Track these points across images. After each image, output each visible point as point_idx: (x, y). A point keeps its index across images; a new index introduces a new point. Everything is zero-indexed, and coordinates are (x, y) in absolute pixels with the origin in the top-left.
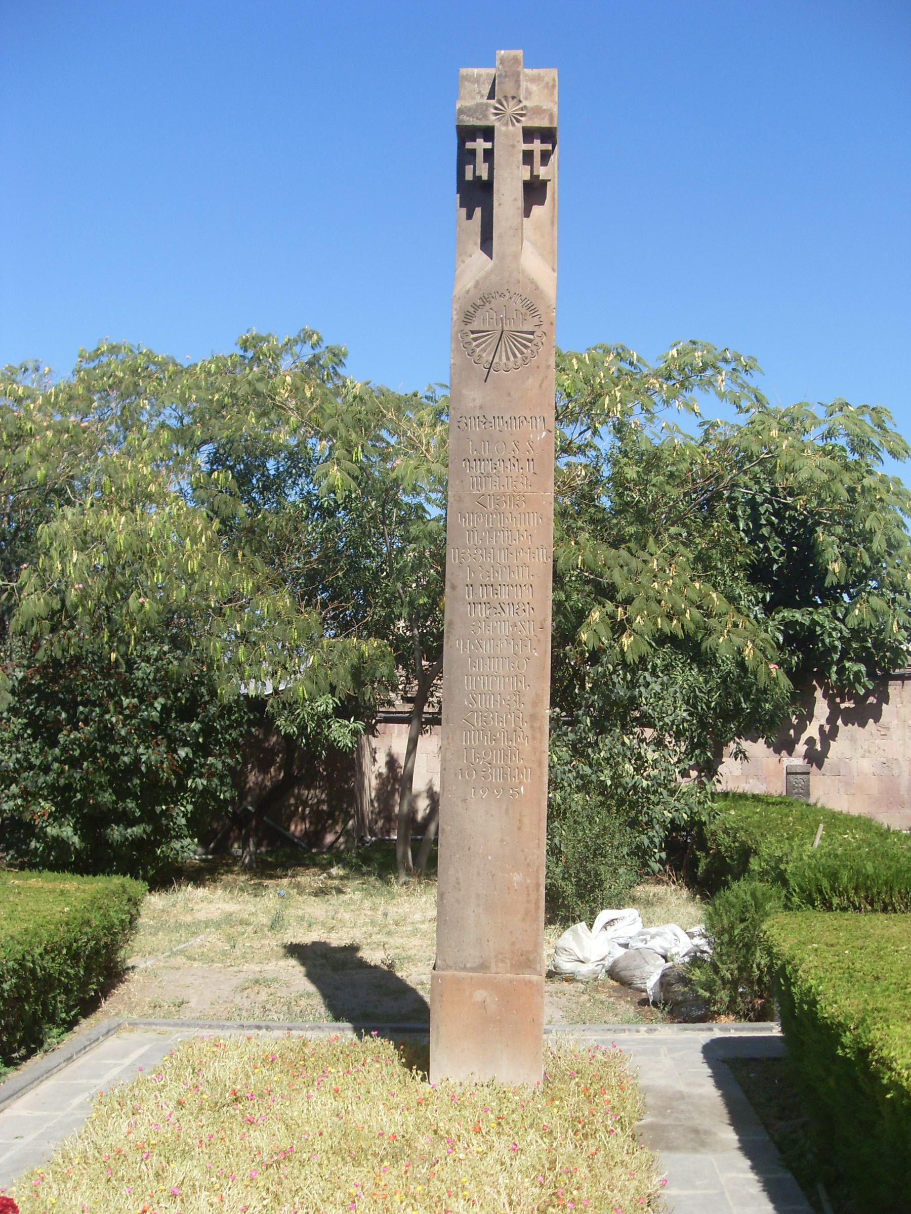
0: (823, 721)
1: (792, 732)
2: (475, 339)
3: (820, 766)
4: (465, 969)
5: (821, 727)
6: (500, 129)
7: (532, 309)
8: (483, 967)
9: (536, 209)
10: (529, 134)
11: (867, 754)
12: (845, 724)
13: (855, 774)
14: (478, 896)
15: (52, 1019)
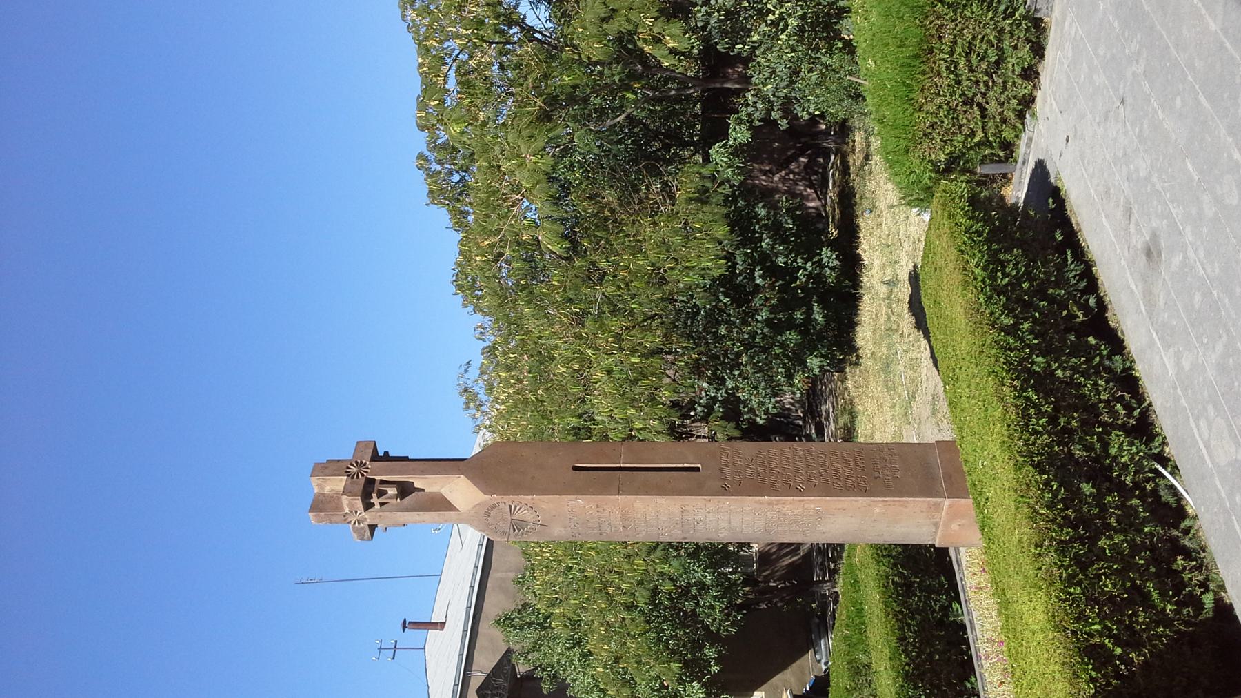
2: (519, 530)
4: (936, 533)
6: (369, 522)
7: (493, 507)
8: (936, 525)
9: (416, 485)
10: (368, 506)
14: (887, 527)
15: (946, 609)
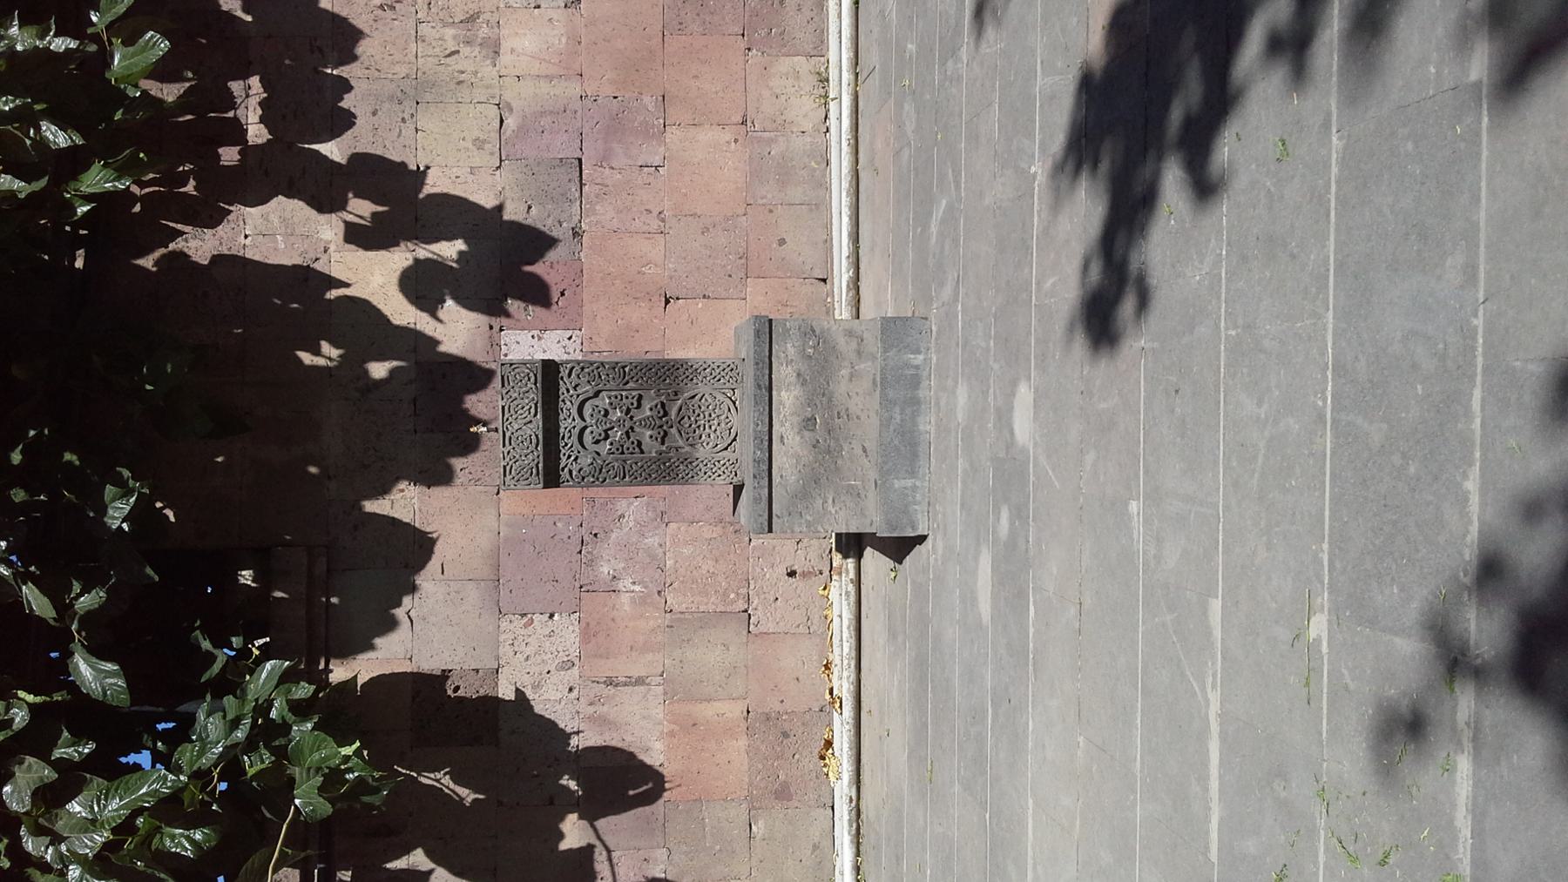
0: (329, 228)
1: (378, 370)
3: (537, 242)
5: (357, 236)
11: (484, 31)
12: (342, 122)
13: (574, 89)
